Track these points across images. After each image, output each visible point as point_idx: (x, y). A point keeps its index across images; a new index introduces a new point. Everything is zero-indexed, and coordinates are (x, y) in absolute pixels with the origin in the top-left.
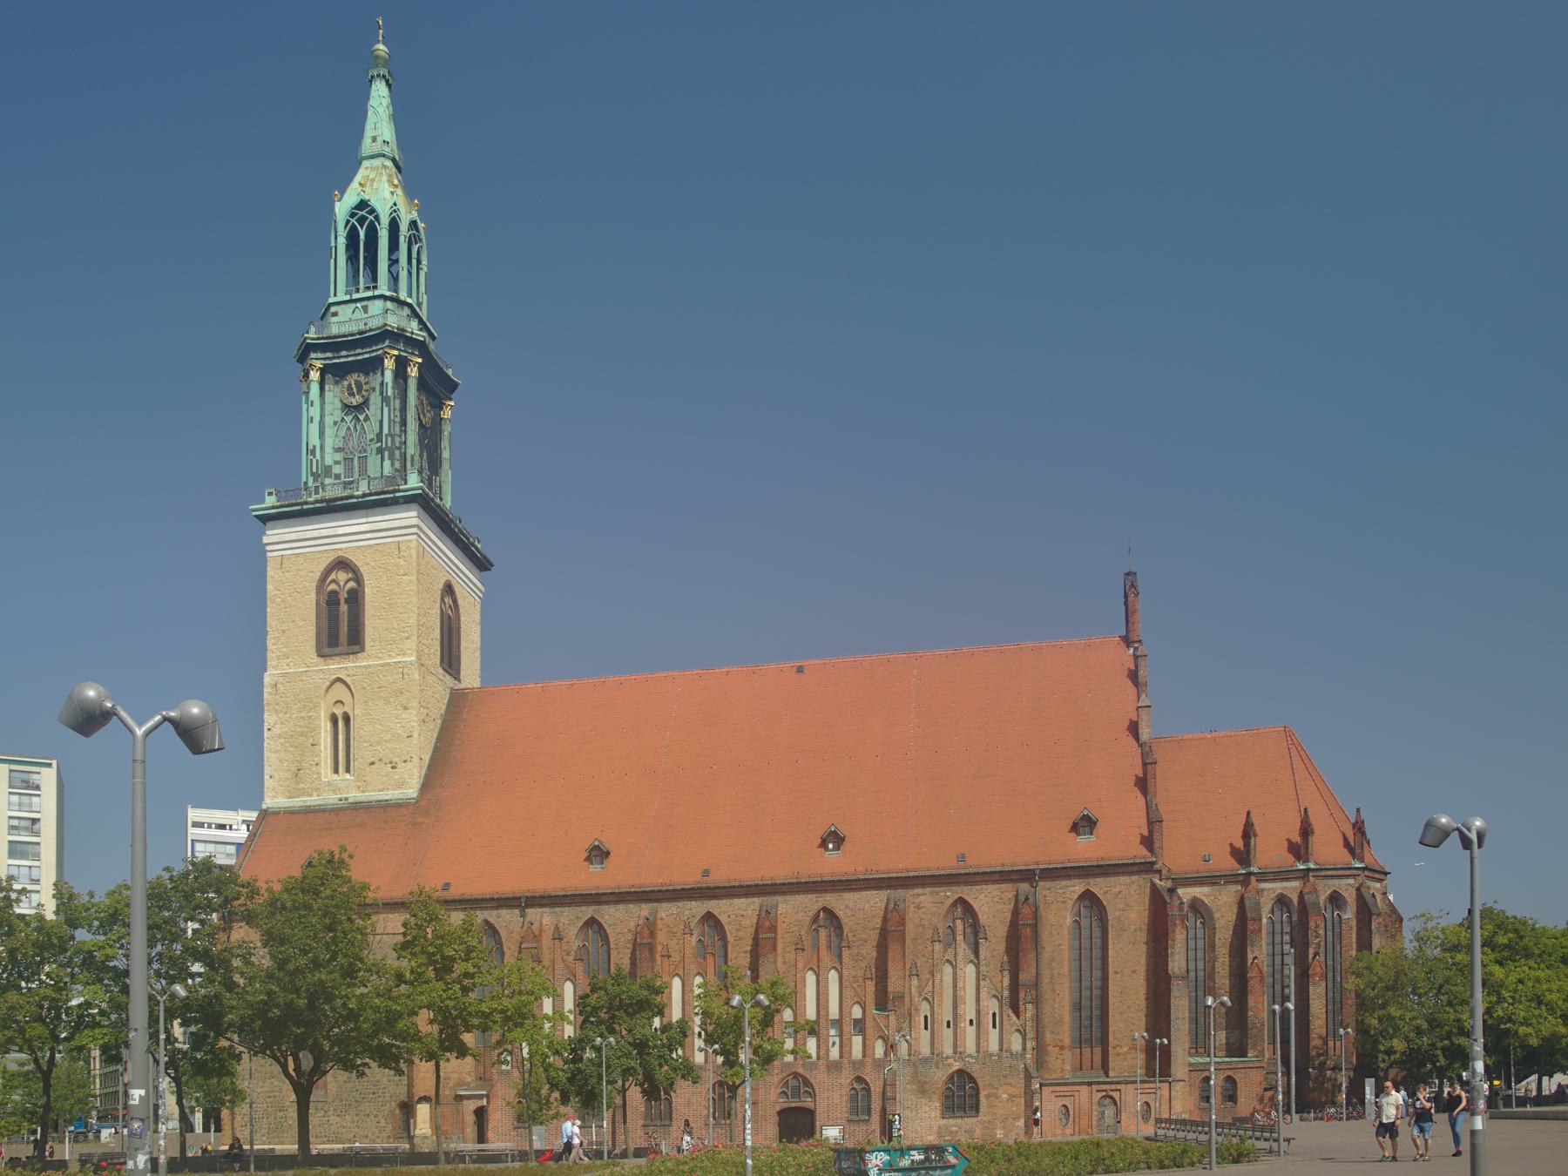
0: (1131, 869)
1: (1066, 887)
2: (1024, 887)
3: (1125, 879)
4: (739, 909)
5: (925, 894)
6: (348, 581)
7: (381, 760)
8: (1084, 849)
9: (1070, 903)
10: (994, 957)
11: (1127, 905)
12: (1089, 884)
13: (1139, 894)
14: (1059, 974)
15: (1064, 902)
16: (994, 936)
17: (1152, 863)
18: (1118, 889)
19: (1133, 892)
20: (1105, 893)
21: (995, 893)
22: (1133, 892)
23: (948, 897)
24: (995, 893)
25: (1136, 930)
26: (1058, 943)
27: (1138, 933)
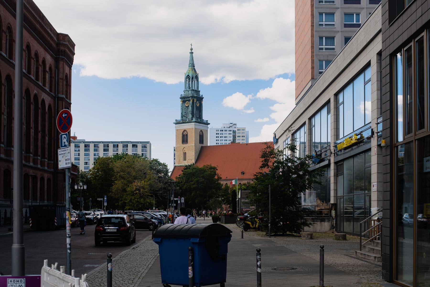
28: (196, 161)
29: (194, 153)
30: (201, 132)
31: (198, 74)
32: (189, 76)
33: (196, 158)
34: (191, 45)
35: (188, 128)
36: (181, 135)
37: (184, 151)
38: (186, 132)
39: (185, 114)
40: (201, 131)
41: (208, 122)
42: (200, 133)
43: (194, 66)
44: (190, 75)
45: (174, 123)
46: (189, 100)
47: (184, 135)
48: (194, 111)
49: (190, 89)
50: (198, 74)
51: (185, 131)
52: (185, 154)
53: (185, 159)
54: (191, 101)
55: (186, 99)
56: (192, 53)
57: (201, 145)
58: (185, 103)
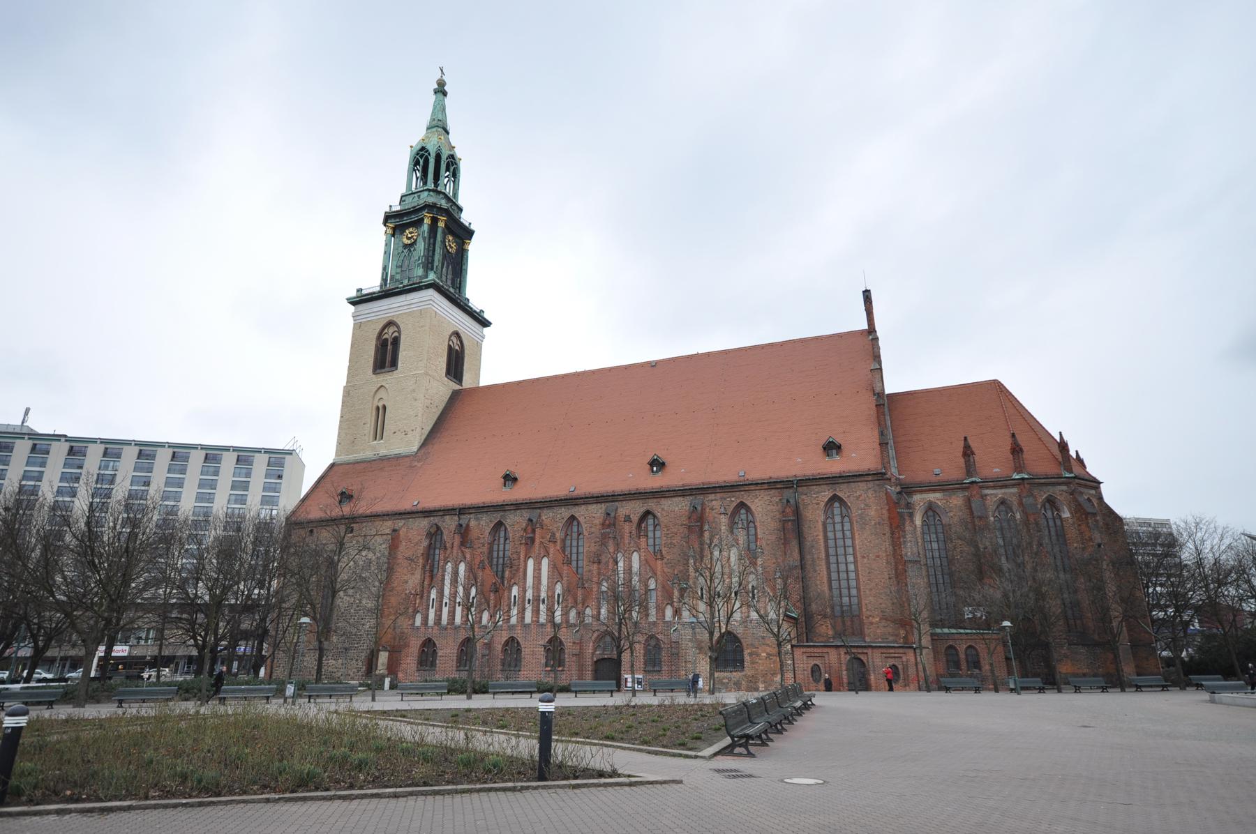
0: (866, 478)
1: (818, 492)
2: (788, 493)
4: (592, 513)
5: (716, 500)
6: (394, 332)
7: (399, 430)
8: (834, 465)
9: (822, 504)
10: (768, 545)
11: (867, 505)
12: (835, 490)
13: (876, 497)
14: (818, 558)
15: (818, 504)
16: (768, 529)
17: (885, 474)
18: (858, 494)
19: (870, 496)
20: (849, 496)
22: (870, 496)
23: (733, 501)
24: (766, 498)
25: (875, 524)
26: (815, 534)
27: (878, 526)
28: (426, 440)
30: (454, 339)
31: (460, 159)
35: (405, 313)
36: (374, 343)
37: (376, 399)
38: (391, 330)
39: (397, 273)
41: (487, 316)
42: (450, 340)
45: (347, 299)
46: (418, 223)
47: (386, 340)
48: (433, 261)
49: (425, 188)
50: (460, 159)
51: (390, 323)
52: (381, 411)
54: (427, 221)
55: (406, 220)
56: (441, 90)
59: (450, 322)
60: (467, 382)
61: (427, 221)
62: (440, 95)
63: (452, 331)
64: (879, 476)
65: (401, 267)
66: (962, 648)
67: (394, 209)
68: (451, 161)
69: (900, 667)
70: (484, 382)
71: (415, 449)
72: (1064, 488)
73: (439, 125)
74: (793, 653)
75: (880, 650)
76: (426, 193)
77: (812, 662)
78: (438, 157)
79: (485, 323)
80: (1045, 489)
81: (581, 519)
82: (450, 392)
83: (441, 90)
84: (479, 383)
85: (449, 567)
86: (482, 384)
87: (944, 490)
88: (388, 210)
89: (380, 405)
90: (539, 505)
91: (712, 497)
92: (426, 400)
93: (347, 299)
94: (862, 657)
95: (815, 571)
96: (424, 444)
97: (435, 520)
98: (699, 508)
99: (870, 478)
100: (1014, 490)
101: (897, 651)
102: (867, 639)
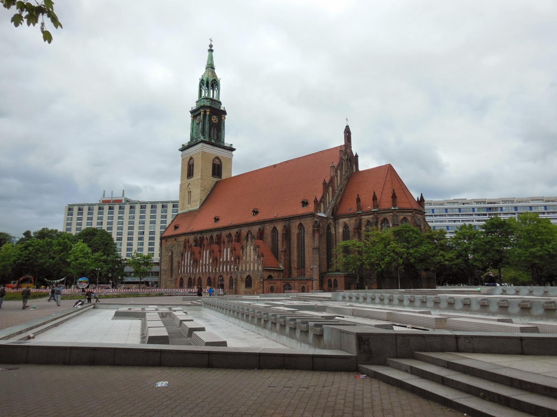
1: (296, 222)
2: (287, 223)
3: (308, 219)
8: (303, 211)
9: (297, 226)
21: (282, 225)
24: (282, 225)
29: (199, 190)
30: (217, 160)
31: (220, 79)
32: (204, 81)
33: (204, 199)
34: (211, 40)
38: (192, 160)
40: (217, 158)
41: (234, 147)
42: (213, 160)
43: (213, 68)
44: (205, 79)
45: (179, 150)
46: (200, 114)
47: (191, 165)
50: (220, 79)
51: (191, 158)
52: (190, 192)
53: (189, 202)
55: (197, 113)
56: (211, 51)
57: (216, 180)
58: (196, 119)
59: (212, 154)
60: (224, 176)
61: (202, 113)
62: (210, 52)
63: (214, 157)
64: (313, 215)
65: (196, 133)
66: (333, 280)
67: (193, 109)
68: (214, 82)
69: (306, 287)
70: (234, 174)
71: (198, 207)
72: (391, 214)
73: (211, 67)
74: (263, 282)
75: (298, 281)
76: (203, 100)
77: (271, 285)
78: (208, 82)
79: (232, 150)
80: (383, 215)
81: (232, 234)
82: (215, 182)
83: (211, 51)
84: (231, 176)
85: (186, 253)
86: (232, 176)
87: (349, 217)
88: (191, 110)
89: (189, 191)
90: (221, 229)
91: (266, 225)
92: (202, 188)
93: (179, 150)
94: (290, 283)
95: (293, 252)
96: (202, 205)
97: (195, 235)
98: (261, 229)
99: (310, 216)
100: (372, 216)
101: (305, 281)
102: (306, 277)
